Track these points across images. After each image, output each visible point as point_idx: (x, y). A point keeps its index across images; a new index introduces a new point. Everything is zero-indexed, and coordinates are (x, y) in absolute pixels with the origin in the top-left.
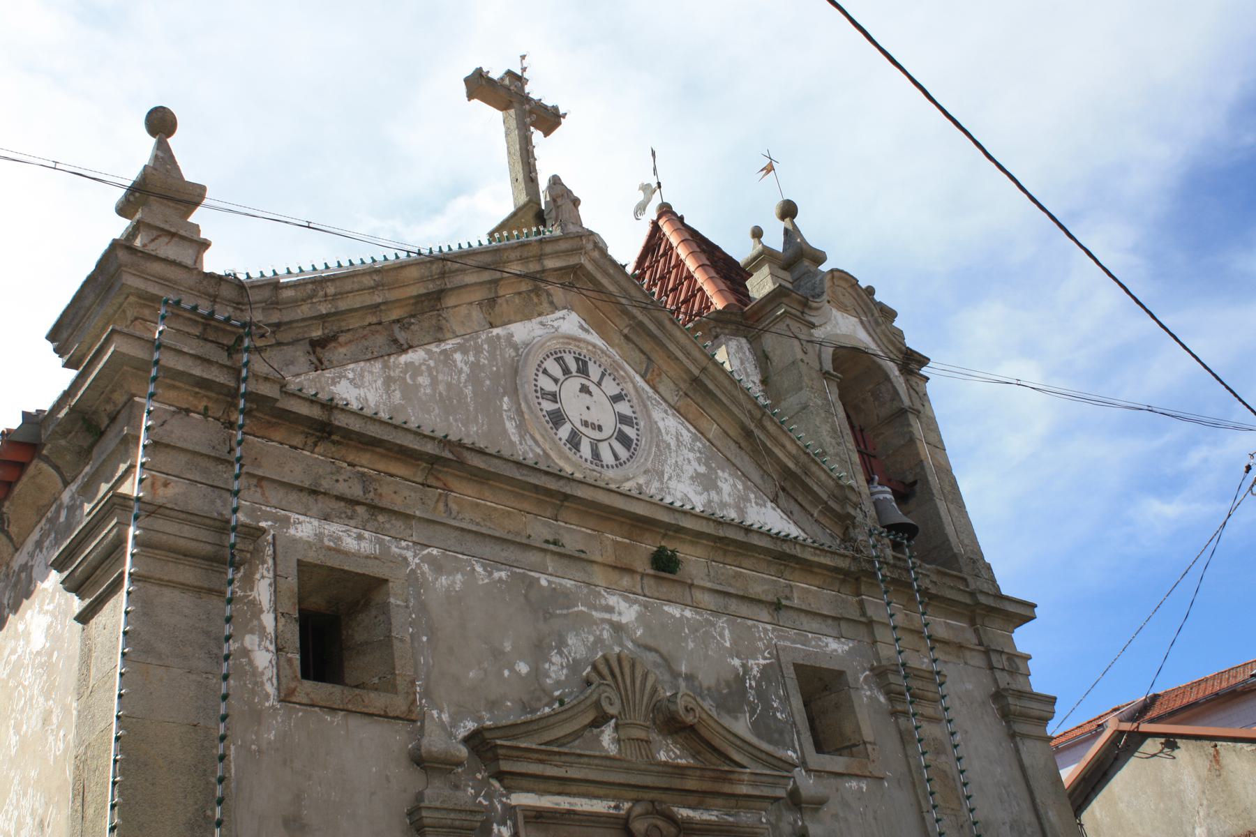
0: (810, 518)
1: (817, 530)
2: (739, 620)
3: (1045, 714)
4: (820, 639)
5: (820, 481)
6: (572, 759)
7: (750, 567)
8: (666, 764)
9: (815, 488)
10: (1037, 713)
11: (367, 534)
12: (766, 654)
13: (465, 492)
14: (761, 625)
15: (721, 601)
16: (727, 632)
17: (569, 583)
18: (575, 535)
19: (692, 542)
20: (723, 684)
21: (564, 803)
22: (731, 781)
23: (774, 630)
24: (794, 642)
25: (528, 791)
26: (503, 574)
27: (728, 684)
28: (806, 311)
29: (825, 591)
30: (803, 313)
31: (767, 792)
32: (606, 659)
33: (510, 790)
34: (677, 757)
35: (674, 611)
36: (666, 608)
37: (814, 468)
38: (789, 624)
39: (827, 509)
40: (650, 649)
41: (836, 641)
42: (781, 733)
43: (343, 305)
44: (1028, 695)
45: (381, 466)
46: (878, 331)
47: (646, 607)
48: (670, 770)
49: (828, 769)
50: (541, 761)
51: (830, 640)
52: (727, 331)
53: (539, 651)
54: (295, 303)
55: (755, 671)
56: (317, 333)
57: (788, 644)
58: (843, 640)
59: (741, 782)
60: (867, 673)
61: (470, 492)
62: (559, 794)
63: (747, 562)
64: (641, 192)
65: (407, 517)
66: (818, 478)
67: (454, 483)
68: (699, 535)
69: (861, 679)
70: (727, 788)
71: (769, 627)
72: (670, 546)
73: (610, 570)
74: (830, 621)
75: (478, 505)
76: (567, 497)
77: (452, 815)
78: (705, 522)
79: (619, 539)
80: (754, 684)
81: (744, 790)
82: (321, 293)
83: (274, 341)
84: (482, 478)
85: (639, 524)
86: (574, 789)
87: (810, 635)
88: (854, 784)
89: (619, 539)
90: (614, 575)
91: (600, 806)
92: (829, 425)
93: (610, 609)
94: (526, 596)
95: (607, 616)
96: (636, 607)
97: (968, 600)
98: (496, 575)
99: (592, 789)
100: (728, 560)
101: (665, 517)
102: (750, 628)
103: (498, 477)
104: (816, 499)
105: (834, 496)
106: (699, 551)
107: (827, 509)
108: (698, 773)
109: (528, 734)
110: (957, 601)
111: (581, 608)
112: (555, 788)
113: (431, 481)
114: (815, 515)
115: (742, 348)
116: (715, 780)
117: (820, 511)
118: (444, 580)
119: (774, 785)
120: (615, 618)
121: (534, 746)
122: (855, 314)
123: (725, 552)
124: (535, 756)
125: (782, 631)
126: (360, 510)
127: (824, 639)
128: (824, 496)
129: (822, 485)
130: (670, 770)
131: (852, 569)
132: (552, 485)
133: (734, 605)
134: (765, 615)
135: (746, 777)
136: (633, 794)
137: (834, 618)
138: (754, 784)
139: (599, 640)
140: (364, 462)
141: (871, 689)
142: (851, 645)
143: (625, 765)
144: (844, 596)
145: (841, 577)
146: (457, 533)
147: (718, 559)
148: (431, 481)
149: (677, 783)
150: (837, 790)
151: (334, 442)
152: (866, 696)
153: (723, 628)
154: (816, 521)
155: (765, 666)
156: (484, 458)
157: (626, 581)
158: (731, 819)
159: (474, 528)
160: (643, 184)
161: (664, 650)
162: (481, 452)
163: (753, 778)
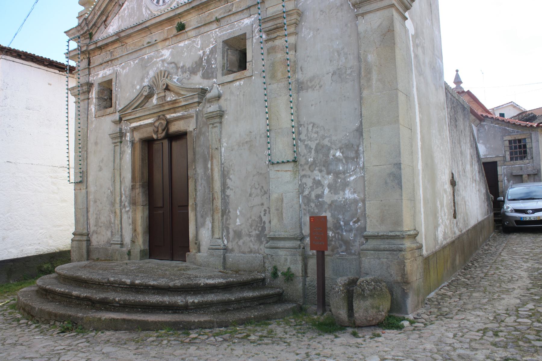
2: (205, 34)
4: (240, 22)
6: (136, 112)
7: (213, 8)
8: (170, 101)
11: (111, 68)
12: (214, 43)
13: (129, 41)
14: (213, 31)
15: (197, 30)
16: (200, 42)
17: (152, 54)
18: (157, 35)
19: (189, 14)
20: (194, 63)
21: (142, 123)
22: (178, 103)
23: (219, 30)
24: (228, 30)
25: (134, 122)
26: (137, 61)
27: (196, 63)
31: (191, 101)
32: (165, 71)
33: (131, 123)
34: (173, 97)
35: (182, 44)
36: (179, 45)
38: (226, 23)
40: (171, 63)
41: (249, 18)
42: (212, 73)
43: (102, 9)
45: (113, 47)
47: (173, 48)
48: (158, 106)
49: (225, 82)
50: (130, 115)
51: (245, 20)
53: (142, 80)
54: (93, 18)
55: (208, 53)
56: (104, 18)
57: (225, 32)
59: (181, 102)
61: (131, 41)
62: (140, 121)
63: (211, 7)
65: (117, 59)
67: (127, 41)
68: (187, 11)
70: (177, 105)
71: (217, 30)
72: (179, 21)
73: (163, 42)
74: (245, 11)
75: (133, 43)
76: (147, 27)
77: (114, 135)
78: (185, 6)
79: (169, 28)
80: (206, 58)
81: (183, 104)
82: (96, 11)
83: (97, 28)
84: (129, 36)
85: (169, 20)
86: (142, 118)
87: (235, 23)
88: (237, 83)
89: (169, 28)
90: (164, 43)
91: (150, 121)
93: (162, 56)
94: (141, 65)
95: (161, 59)
96: (170, 50)
98: (135, 62)
99: (145, 117)
100: (204, 11)
101: (172, 14)
102: (209, 35)
103: (132, 33)
106: (194, 14)
108: (167, 104)
109: (128, 109)
111: (155, 60)
112: (138, 120)
113: (123, 44)
116: (173, 104)
118: (124, 71)
119: (193, 98)
120: (163, 58)
121: (130, 111)
123: (202, 9)
124: (128, 114)
125: (223, 28)
126: (110, 62)
127: (242, 21)
130: (158, 106)
132: (139, 28)
133: (203, 30)
134: (214, 26)
135: (181, 100)
136: (156, 115)
137: (246, 9)
138: (186, 101)
139: (158, 68)
140: (110, 49)
143: (147, 109)
146: (127, 56)
147: (201, 13)
148: (123, 44)
149: (162, 109)
150: (230, 88)
151: (104, 48)
153: (199, 41)
155: (212, 48)
156: (124, 32)
157: (167, 43)
158: (186, 113)
159: (133, 51)
161: (176, 62)
162: (123, 31)
163: (184, 99)
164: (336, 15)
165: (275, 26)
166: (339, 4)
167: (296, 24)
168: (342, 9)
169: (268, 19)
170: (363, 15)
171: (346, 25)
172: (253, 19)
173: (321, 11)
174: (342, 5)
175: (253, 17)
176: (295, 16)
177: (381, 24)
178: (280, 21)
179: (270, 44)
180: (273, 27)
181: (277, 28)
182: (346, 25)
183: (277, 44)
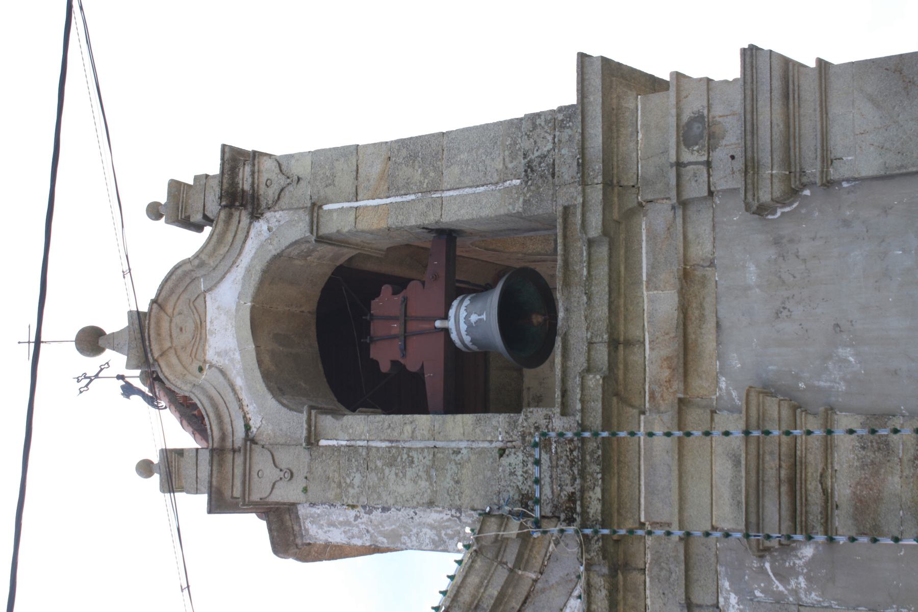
0: (539, 585)
1: (556, 574)
3: (777, 72)
5: (482, 583)
9: (494, 591)
10: (778, 107)
28: (229, 444)
29: (648, 602)
30: (234, 451)
37: (466, 597)
39: (521, 561)
44: (749, 137)
46: (212, 263)
52: (296, 528)
58: (721, 600)
60: (767, 565)
64: (132, 397)
66: (479, 587)
69: (781, 588)
92: (387, 471)
97: (603, 251)
104: (512, 580)
105: (497, 557)
107: (521, 561)
110: (610, 278)
114: (534, 576)
115: (312, 516)
117: (525, 570)
122: (202, 297)
128: (501, 576)
129: (485, 583)
131: (605, 570)
141: (793, 572)
142: (727, 584)
144: (649, 556)
145: (620, 576)
152: (808, 591)
154: (541, 573)
160: (122, 394)
164: (805, 260)
165: (784, 489)
166: (772, 253)
167: (797, 407)
168: (791, 241)
169: (753, 509)
170: (827, 160)
171: (846, 223)
172: (733, 599)
173: (777, 314)
174: (777, 242)
175: (727, 599)
176: (772, 406)
177: (871, 99)
178: (771, 464)
179: (842, 523)
180: (785, 499)
181: (792, 482)
182: (846, 223)
183: (848, 491)
